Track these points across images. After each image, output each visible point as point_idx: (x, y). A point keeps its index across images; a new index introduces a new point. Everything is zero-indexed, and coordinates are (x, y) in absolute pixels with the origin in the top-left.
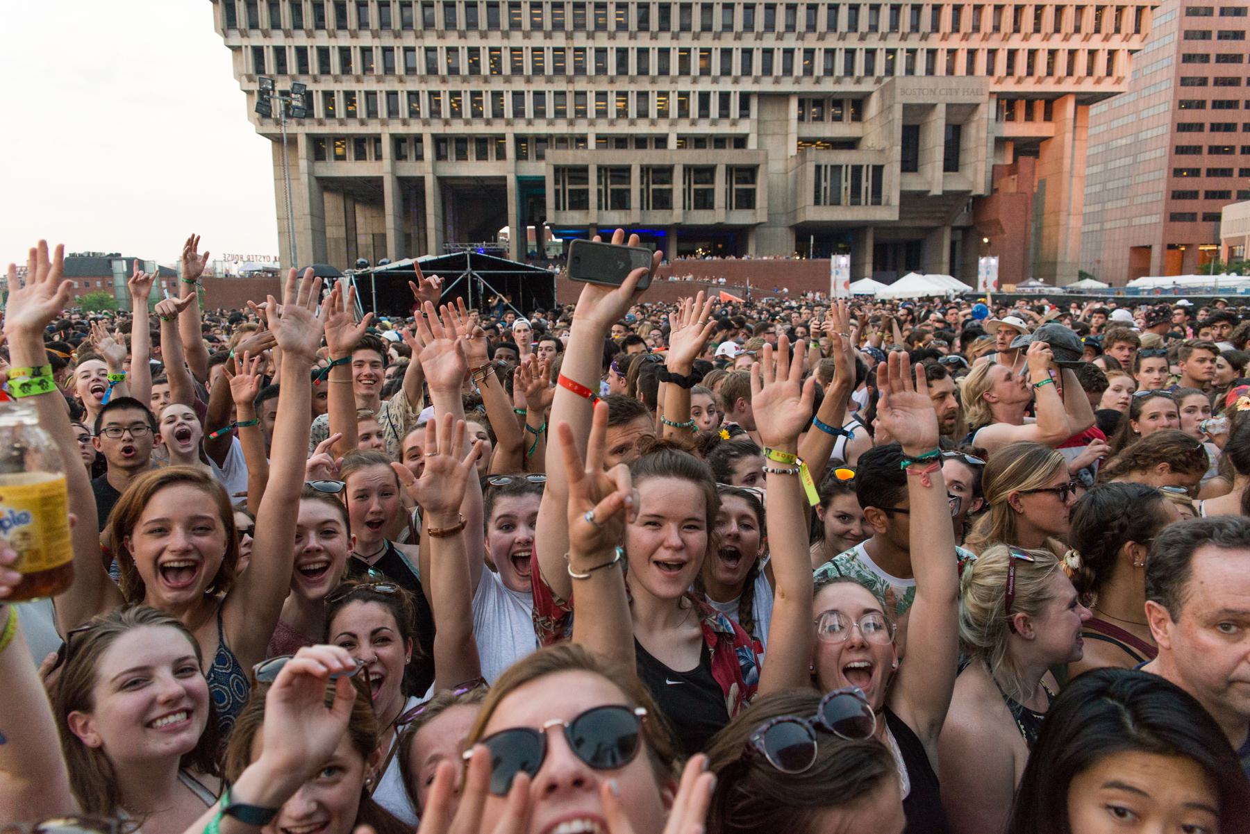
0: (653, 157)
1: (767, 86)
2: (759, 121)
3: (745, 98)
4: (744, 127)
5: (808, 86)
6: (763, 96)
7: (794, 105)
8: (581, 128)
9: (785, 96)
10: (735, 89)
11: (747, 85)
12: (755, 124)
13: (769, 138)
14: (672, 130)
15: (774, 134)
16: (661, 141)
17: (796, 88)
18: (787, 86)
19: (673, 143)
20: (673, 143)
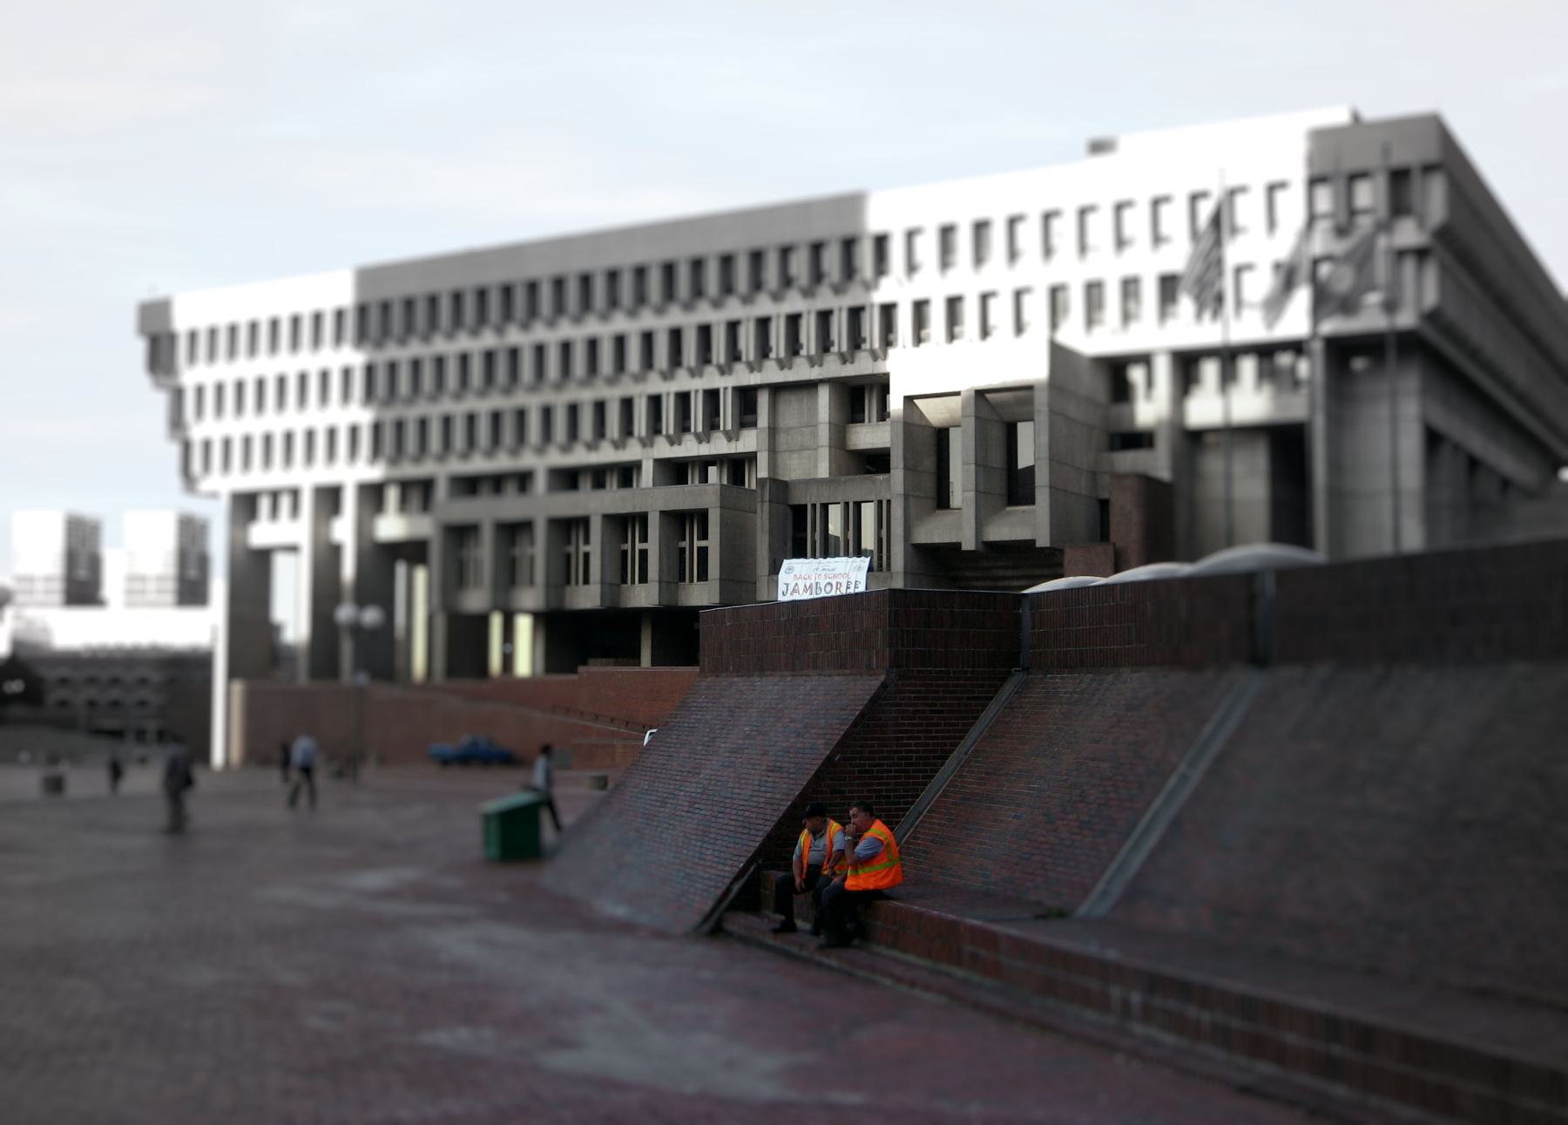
0: (613, 500)
1: (772, 373)
2: (773, 430)
3: (746, 396)
4: (749, 441)
5: (833, 368)
6: (777, 390)
7: (824, 396)
8: (527, 460)
9: (810, 386)
10: (725, 383)
11: (743, 376)
12: (765, 436)
13: (795, 455)
14: (646, 454)
15: (803, 449)
16: (627, 473)
17: (814, 373)
18: (801, 371)
19: (648, 469)
20: (648, 469)
